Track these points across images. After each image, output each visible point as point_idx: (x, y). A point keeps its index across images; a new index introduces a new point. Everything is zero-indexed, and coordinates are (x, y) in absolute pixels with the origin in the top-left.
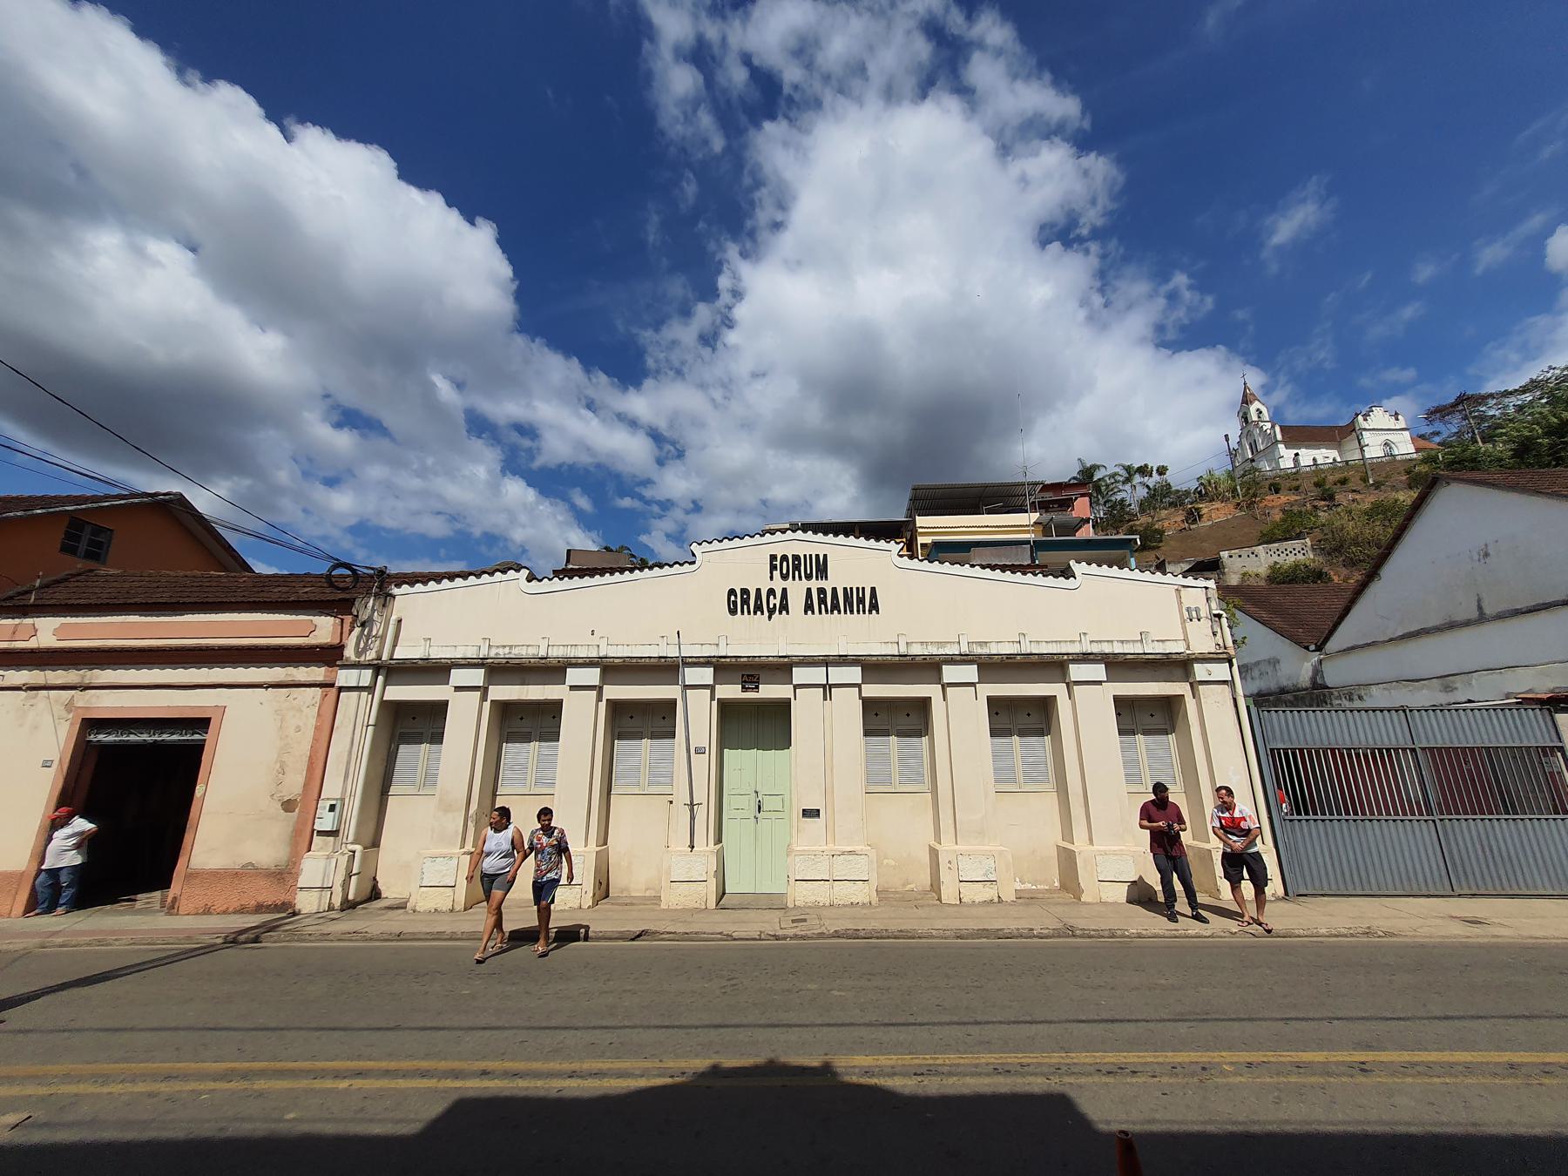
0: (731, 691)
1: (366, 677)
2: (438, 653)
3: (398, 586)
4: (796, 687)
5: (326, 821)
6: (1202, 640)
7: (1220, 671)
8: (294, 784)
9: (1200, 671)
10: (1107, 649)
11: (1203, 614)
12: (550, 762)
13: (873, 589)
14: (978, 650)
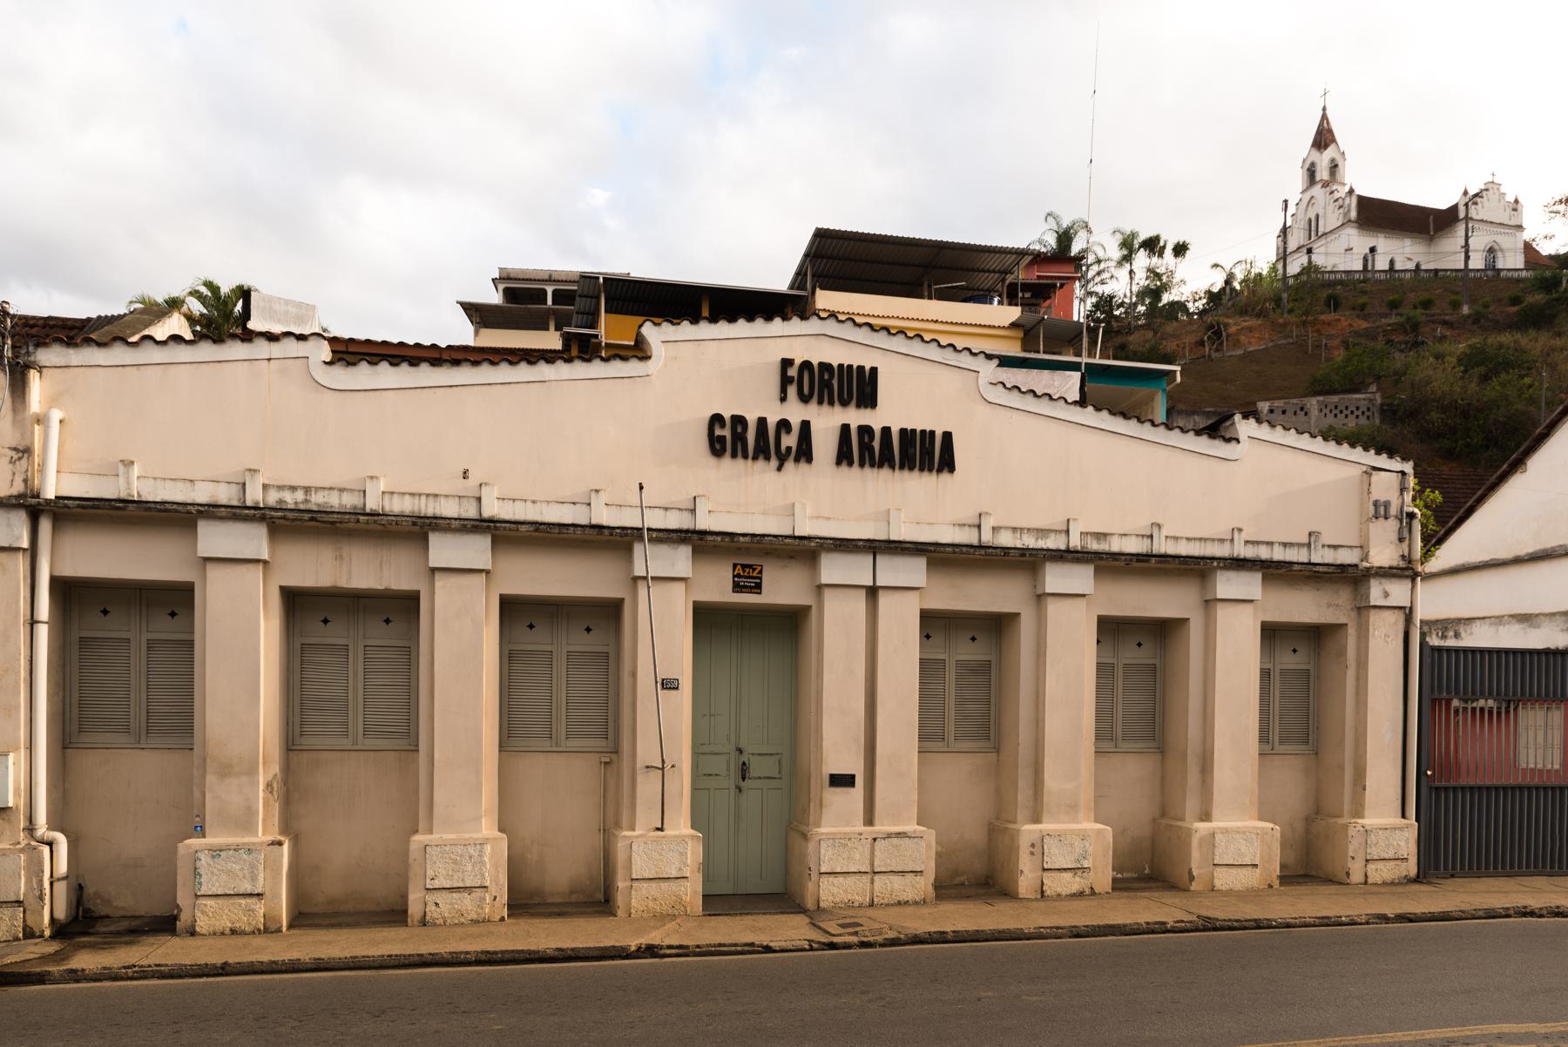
9: (1376, 592)
10: (1264, 553)
13: (947, 436)
14: (1094, 546)
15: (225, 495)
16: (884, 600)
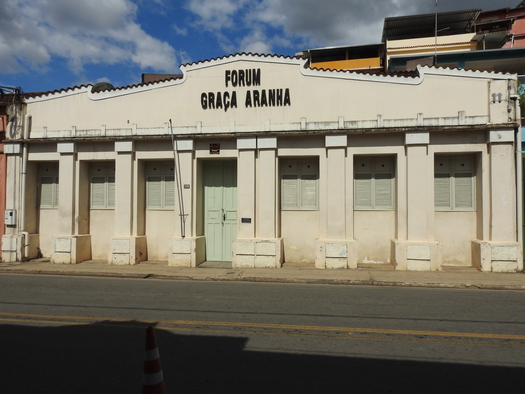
0: (204, 154)
1: (17, 148)
2: (52, 135)
3: (27, 98)
5: (9, 221)
7: (508, 135)
9: (494, 136)
10: (434, 123)
11: (503, 98)
12: (111, 194)
13: (287, 91)
14: (350, 126)
15: (67, 135)
16: (261, 153)
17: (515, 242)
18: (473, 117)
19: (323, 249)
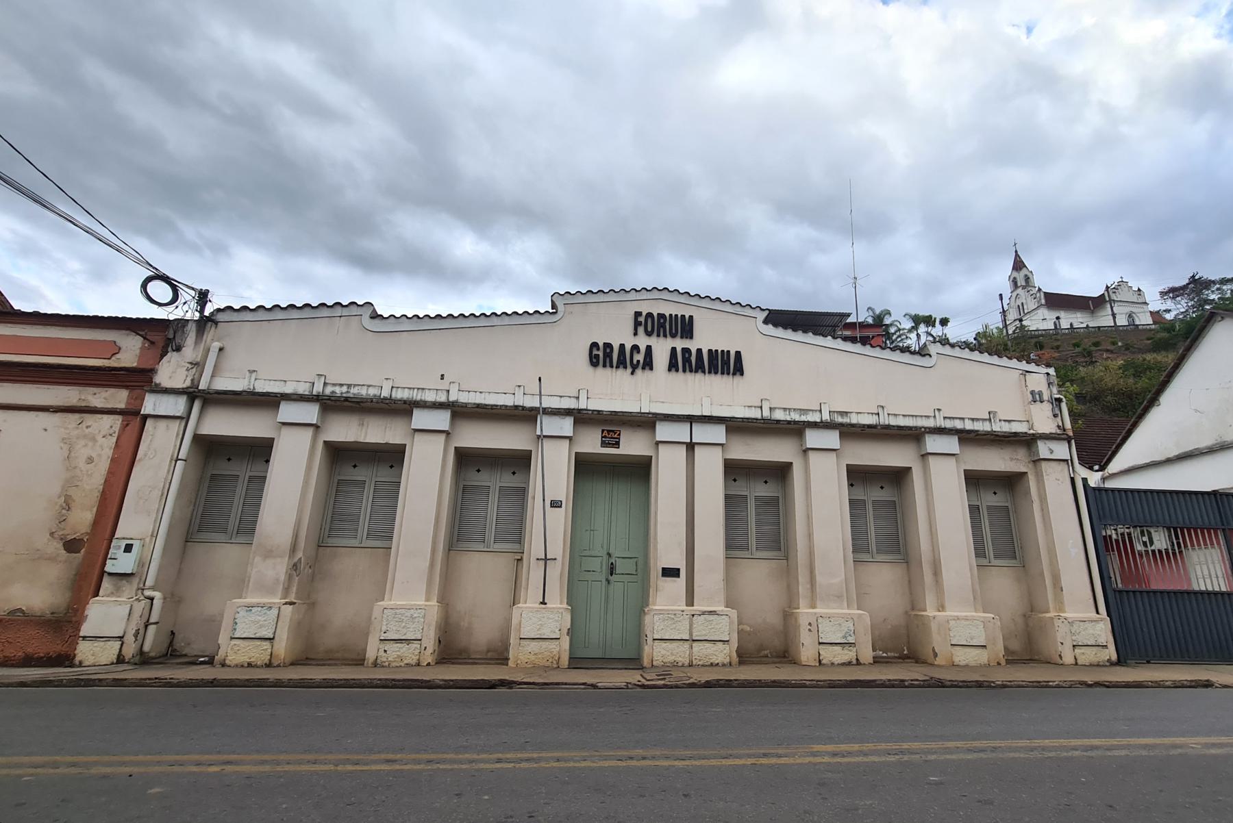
4: (658, 443)
6: (1043, 420)
8: (82, 519)
9: (1043, 449)
10: (959, 425)
11: (1046, 397)
13: (738, 354)
14: (839, 419)
15: (303, 389)
17: (1094, 615)
18: (1009, 421)
19: (814, 628)
